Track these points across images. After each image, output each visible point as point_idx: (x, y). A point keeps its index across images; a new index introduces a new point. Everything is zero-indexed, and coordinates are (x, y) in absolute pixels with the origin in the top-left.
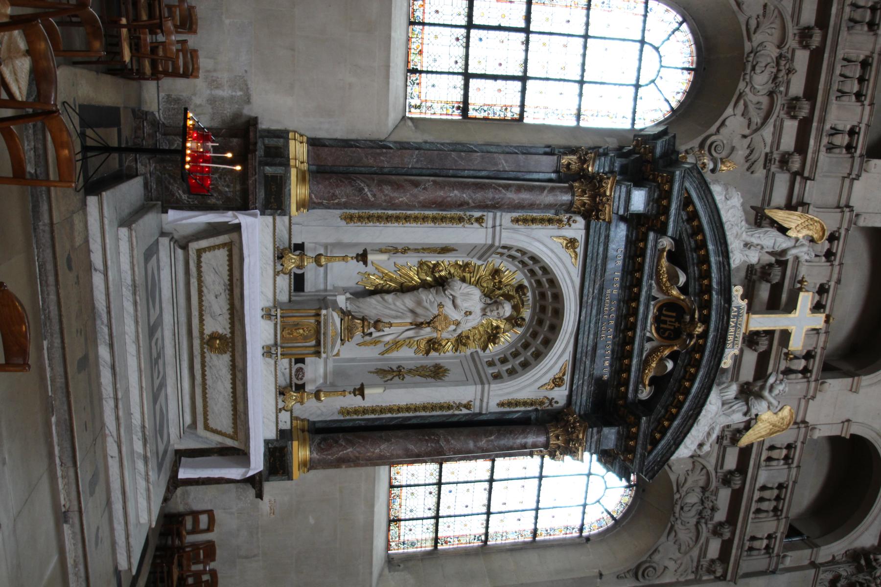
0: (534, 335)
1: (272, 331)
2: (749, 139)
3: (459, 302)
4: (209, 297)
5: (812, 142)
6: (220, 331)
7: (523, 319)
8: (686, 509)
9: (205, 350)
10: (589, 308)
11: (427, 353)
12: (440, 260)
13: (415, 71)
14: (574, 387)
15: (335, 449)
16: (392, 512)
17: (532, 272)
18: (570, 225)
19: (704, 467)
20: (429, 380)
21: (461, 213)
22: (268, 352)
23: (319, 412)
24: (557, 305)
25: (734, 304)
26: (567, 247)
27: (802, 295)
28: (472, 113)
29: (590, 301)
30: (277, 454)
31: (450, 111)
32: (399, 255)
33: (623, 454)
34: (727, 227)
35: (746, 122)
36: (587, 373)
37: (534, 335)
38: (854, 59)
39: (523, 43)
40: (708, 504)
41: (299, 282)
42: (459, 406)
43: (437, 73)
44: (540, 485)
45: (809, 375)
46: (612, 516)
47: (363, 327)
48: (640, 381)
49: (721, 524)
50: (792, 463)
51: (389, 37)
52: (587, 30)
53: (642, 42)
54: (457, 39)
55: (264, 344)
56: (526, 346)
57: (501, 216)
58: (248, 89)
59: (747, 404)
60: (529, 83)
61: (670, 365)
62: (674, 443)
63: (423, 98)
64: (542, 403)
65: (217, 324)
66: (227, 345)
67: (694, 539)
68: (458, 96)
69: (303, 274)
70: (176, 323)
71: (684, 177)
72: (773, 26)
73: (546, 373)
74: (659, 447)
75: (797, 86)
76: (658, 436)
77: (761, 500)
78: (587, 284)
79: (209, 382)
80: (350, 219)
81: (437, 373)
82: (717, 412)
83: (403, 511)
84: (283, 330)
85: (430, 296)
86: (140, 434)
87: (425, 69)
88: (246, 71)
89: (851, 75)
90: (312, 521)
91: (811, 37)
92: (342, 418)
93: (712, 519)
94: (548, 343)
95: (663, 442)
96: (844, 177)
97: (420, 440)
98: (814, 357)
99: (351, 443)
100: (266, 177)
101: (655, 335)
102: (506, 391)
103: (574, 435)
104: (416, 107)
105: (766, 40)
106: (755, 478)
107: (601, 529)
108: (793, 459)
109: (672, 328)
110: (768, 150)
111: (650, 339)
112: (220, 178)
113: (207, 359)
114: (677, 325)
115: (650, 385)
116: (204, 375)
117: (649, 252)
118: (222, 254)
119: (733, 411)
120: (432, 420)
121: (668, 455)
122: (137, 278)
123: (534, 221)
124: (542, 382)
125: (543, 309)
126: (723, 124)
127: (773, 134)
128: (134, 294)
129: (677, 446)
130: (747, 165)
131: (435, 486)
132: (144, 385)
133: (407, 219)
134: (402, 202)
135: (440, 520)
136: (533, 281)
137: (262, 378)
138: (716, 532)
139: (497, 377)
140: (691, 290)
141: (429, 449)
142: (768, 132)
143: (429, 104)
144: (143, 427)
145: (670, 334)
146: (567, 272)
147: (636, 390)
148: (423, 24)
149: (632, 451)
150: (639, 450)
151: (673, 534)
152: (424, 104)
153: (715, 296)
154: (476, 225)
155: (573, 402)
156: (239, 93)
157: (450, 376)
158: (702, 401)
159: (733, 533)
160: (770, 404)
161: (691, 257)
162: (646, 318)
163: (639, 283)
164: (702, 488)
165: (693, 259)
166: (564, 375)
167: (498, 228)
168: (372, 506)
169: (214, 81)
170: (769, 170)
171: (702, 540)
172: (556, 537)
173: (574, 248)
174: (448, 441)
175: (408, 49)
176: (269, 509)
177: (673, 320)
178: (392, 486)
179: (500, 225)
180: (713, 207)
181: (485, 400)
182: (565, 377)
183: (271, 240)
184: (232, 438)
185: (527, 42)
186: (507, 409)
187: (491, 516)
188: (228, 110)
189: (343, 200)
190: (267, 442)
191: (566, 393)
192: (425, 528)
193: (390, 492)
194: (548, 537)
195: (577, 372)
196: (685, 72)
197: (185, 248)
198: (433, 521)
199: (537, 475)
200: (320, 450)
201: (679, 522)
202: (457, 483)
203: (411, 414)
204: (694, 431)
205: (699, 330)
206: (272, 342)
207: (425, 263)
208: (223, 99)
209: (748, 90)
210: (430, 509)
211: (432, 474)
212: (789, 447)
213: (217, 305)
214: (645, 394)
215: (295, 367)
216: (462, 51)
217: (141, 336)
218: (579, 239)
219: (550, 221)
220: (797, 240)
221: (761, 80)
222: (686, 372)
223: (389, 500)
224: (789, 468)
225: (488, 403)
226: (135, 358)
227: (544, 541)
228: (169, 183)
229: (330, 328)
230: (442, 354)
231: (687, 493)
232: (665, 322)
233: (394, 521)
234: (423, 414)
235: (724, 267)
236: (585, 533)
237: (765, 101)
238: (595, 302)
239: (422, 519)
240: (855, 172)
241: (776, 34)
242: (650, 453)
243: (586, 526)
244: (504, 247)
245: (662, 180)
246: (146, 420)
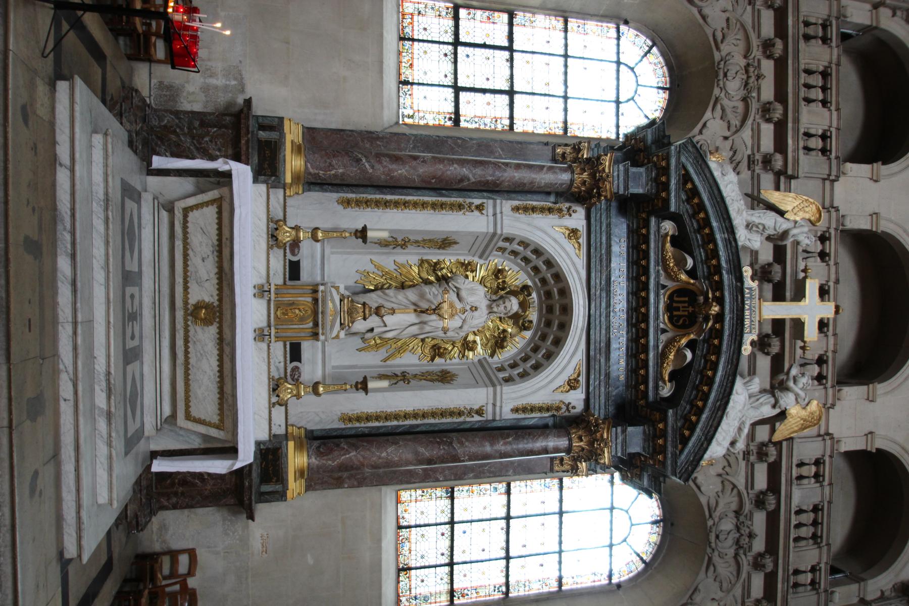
0: (544, 337)
1: (265, 312)
2: (729, 142)
3: (463, 294)
4: (195, 260)
5: (790, 141)
6: (207, 299)
7: (531, 322)
8: (722, 537)
9: (189, 323)
10: (598, 301)
11: (432, 359)
12: (441, 258)
13: (406, 83)
14: (591, 388)
15: (336, 453)
16: (401, 559)
17: (536, 269)
18: (570, 215)
19: (734, 486)
20: (437, 383)
21: (461, 200)
22: (261, 335)
23: (317, 419)
24: (564, 301)
25: (746, 285)
26: (569, 238)
27: (808, 282)
28: (463, 124)
29: (598, 293)
30: (270, 457)
32: (399, 250)
33: (652, 458)
34: (728, 201)
35: (725, 125)
36: (603, 372)
37: (544, 337)
38: (814, 69)
39: (507, 60)
40: (745, 531)
41: (294, 270)
42: (470, 412)
43: (428, 85)
44: (561, 523)
45: (824, 381)
46: (642, 559)
47: (364, 312)
48: (659, 377)
49: (760, 555)
50: (824, 480)
51: (381, 35)
52: (566, 49)
53: (618, 63)
54: (446, 55)
55: (256, 326)
56: (536, 349)
57: (501, 203)
58: (242, 79)
59: (774, 396)
60: (517, 97)
61: (689, 355)
62: (706, 438)
64: (558, 409)
65: (204, 291)
66: (214, 313)
67: (735, 573)
68: (451, 108)
69: (298, 262)
70: (157, 291)
71: (679, 152)
72: (738, 37)
73: (560, 373)
74: (690, 444)
75: (768, 92)
76: (687, 433)
77: (799, 526)
78: (593, 275)
79: (192, 361)
80: (347, 203)
81: (445, 378)
82: (745, 405)
83: (413, 557)
84: (277, 308)
85: (434, 289)
86: (104, 384)
87: (416, 81)
88: (241, 62)
89: (814, 84)
90: (310, 561)
91: (773, 45)
92: (343, 426)
93: (750, 548)
94: (559, 342)
95: (693, 439)
96: (824, 179)
97: (431, 442)
98: (826, 362)
99: (356, 447)
100: (260, 141)
101: (669, 325)
102: (519, 394)
103: (598, 435)
104: (409, 117)
105: (732, 50)
106: (789, 497)
107: (631, 575)
108: (823, 476)
109: (686, 313)
110: (749, 152)
111: (664, 331)
112: (211, 141)
113: (191, 333)
114: (691, 309)
115: (670, 381)
116: (186, 352)
117: (652, 237)
118: (211, 211)
119: (761, 404)
120: (443, 427)
121: (701, 453)
122: (110, 190)
123: (534, 209)
124: (556, 385)
125: (550, 309)
126: (705, 125)
127: (752, 137)
128: (106, 209)
129: (709, 442)
131: (447, 526)
132: (112, 320)
133: (406, 204)
134: (401, 174)
135: (455, 567)
136: (537, 280)
137: (254, 366)
139: (508, 380)
140: (700, 273)
141: (442, 452)
142: (747, 134)
143: (421, 114)
144: (108, 373)
145: (684, 321)
146: (572, 262)
147: (656, 387)
148: (413, 40)
149: (663, 450)
150: (670, 449)
151: (712, 568)
152: (416, 114)
153: (725, 276)
154: (476, 213)
155: (592, 406)
156: (233, 83)
157: (459, 380)
158: (728, 390)
160: (797, 396)
162: (657, 309)
163: (646, 271)
164: (736, 512)
165: (698, 241)
166: (579, 375)
167: (499, 216)
168: (379, 541)
169: (207, 70)
170: (754, 171)
171: (744, 575)
172: (584, 585)
173: (577, 239)
174: (462, 443)
175: (399, 63)
176: (260, 546)
177: (686, 305)
178: (400, 527)
179: (501, 213)
180: (711, 181)
181: (498, 404)
182: (580, 378)
183: (265, 210)
184: (217, 427)
185: (511, 60)
186: (522, 416)
187: (511, 561)
188: (222, 99)
189: (341, 171)
190: (258, 444)
191: (583, 396)
192: (439, 578)
193: (398, 535)
194: (574, 587)
195: (592, 372)
196: (661, 91)
197: (171, 210)
198: (447, 569)
199: (557, 510)
200: (319, 454)
201: (716, 553)
202: (471, 521)
203: (419, 422)
204: (724, 425)
205: (715, 309)
206: (264, 324)
207: (427, 261)
208: (216, 87)
209: (722, 95)
210: (443, 554)
211: (443, 512)
212: (818, 462)
213: (204, 269)
214: (666, 391)
215: (290, 366)
216: (450, 67)
217: (111, 259)
218: (580, 229)
219: (550, 210)
220: (796, 222)
221: (734, 86)
222: (706, 361)
223: (397, 544)
224: (821, 486)
225: (501, 407)
226: (103, 288)
227: (571, 590)
228: (156, 144)
229: (330, 305)
230: (448, 361)
231: (720, 519)
232: (678, 309)
233: (404, 569)
234: (432, 421)
235: (730, 243)
236: (615, 580)
237: (740, 105)
238: (604, 295)
239: (435, 566)
240: (834, 173)
241: (742, 45)
242: (681, 451)
243: (615, 571)
244: (508, 239)
245: (658, 160)
246: (112, 365)
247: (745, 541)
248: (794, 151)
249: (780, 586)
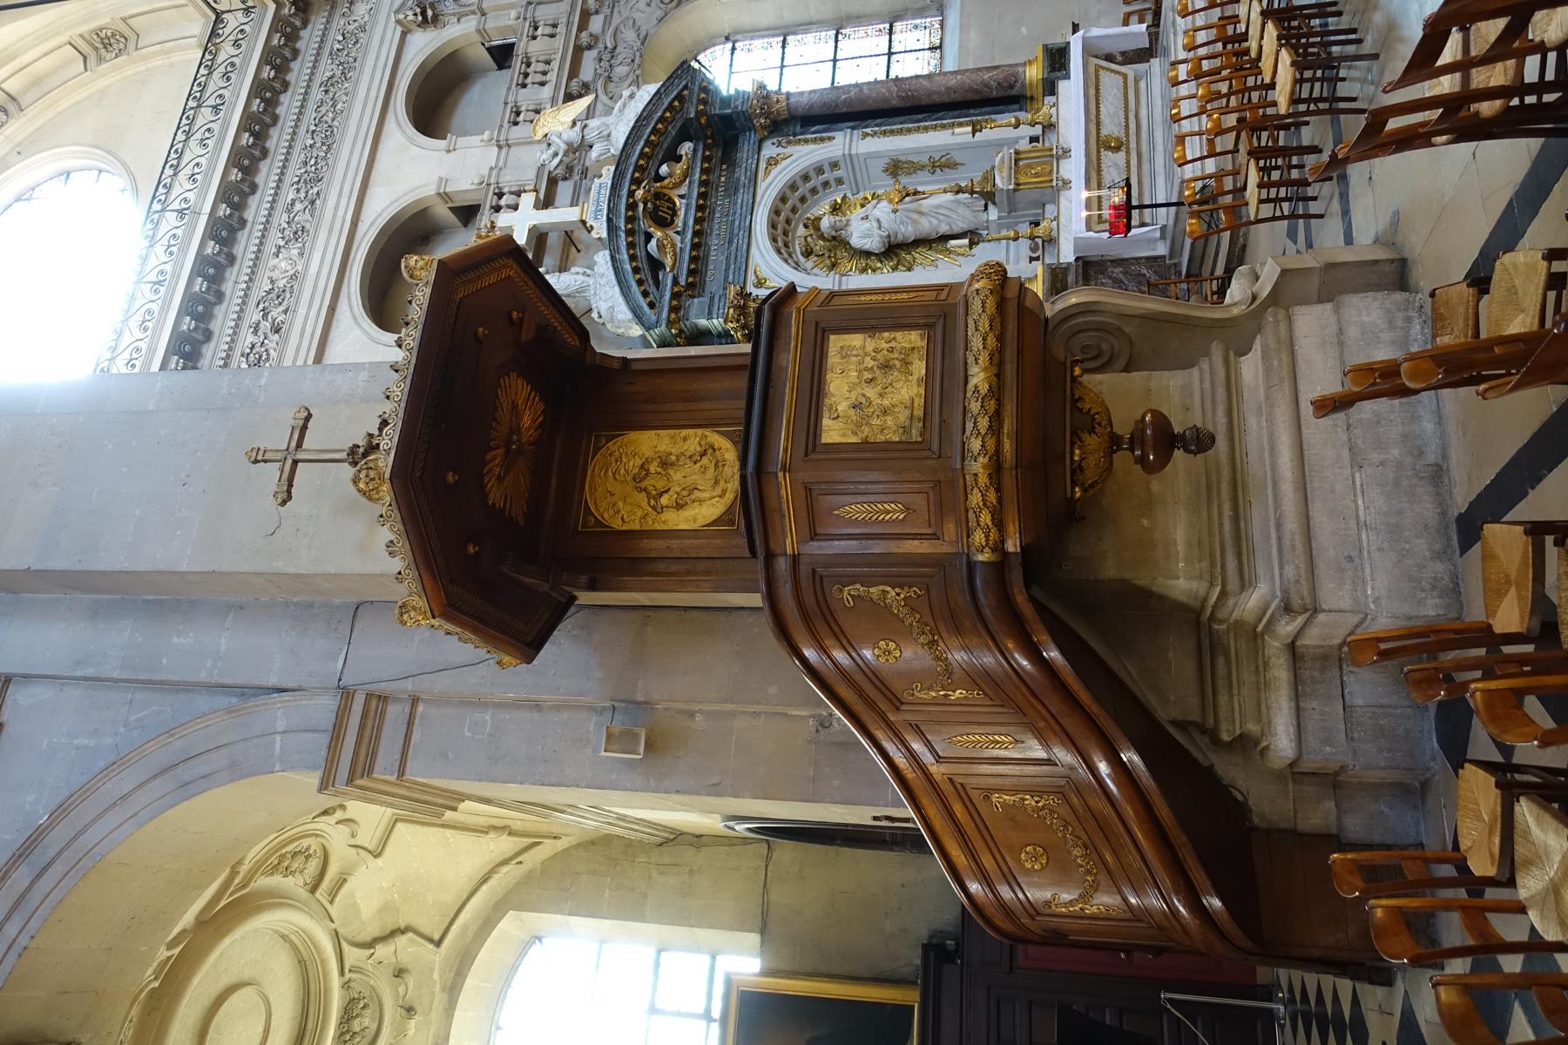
0: (794, 210)
3: (875, 225)
22: (1066, 152)
42: (874, 134)
49: (589, 47)
56: (803, 200)
70: (1151, 160)
77: (545, 73)
81: (896, 168)
111: (681, 197)
116: (1127, 118)
138: (595, 38)
139: (835, 165)
147: (695, 150)
159: (577, 37)
161: (643, 264)
190: (1067, 77)
200: (1015, 75)
204: (641, 106)
214: (686, 148)
236: (729, 45)
242: (686, 87)
247: (606, 56)
249: (577, 20)
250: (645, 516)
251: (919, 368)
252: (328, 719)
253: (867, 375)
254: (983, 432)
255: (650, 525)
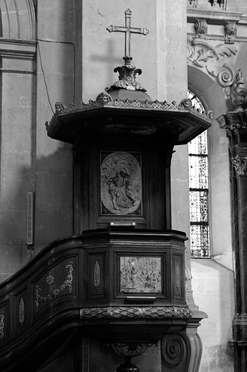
2: (219, 56)
31: (205, 232)
35: (210, 59)
58: (214, 347)
63: (200, 248)
104: (205, 252)
110: (223, 42)
126: (211, 74)
130: (233, 55)
170: (235, 41)
237: (198, 48)
248: (227, 16)
250: (106, 178)
251: (147, 290)
252: (23, 38)
253: (145, 272)
254: (121, 313)
255: (102, 180)
